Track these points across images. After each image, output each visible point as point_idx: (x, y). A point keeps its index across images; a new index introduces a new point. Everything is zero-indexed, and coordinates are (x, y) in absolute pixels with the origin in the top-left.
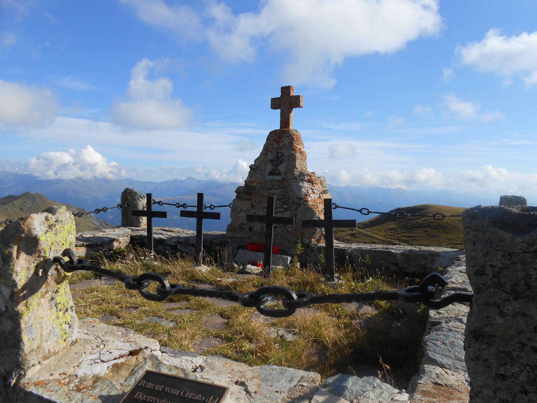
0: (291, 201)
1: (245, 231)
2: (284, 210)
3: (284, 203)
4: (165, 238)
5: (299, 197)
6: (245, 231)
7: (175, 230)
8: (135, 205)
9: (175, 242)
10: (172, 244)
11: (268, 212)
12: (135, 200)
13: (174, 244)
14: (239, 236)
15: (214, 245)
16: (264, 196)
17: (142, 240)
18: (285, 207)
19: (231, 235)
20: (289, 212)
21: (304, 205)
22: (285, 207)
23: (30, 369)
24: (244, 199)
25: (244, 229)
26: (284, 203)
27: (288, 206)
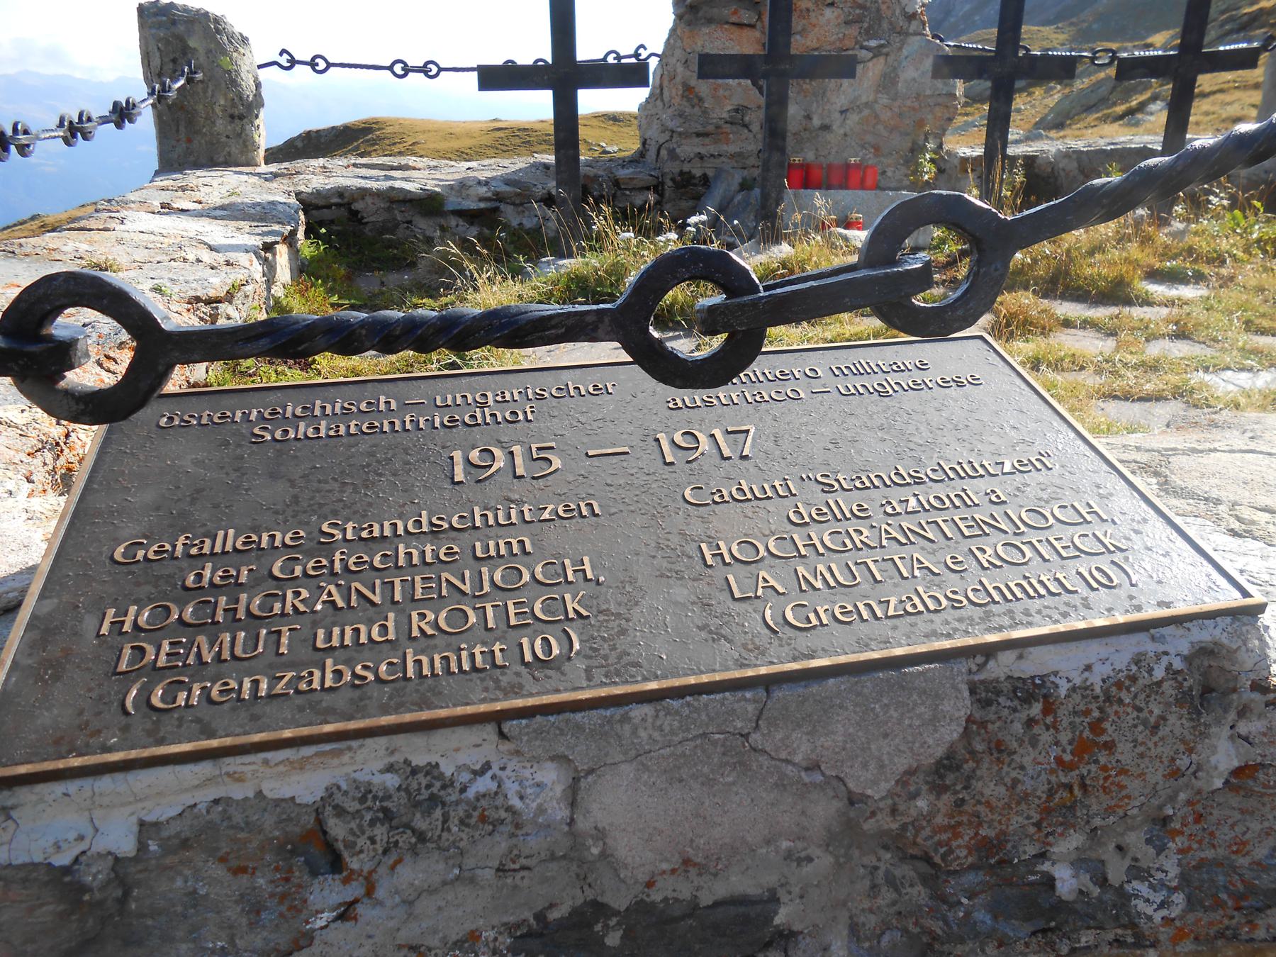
0: (885, 25)
1: (750, 131)
2: (871, 55)
3: (867, 31)
4: (437, 189)
5: (909, 10)
6: (750, 131)
7: (419, 165)
8: (229, 72)
9: (481, 199)
10: (473, 205)
11: (1000, 41)
12: (224, 52)
13: (482, 205)
14: (732, 149)
15: (628, 193)
16: (801, 11)
17: (349, 204)
18: (873, 43)
19: (703, 151)
20: (882, 59)
21: (918, 38)
22: (873, 43)
23: (797, 943)
24: (733, 24)
25: (746, 126)
26: (869, 33)
27: (882, 42)
